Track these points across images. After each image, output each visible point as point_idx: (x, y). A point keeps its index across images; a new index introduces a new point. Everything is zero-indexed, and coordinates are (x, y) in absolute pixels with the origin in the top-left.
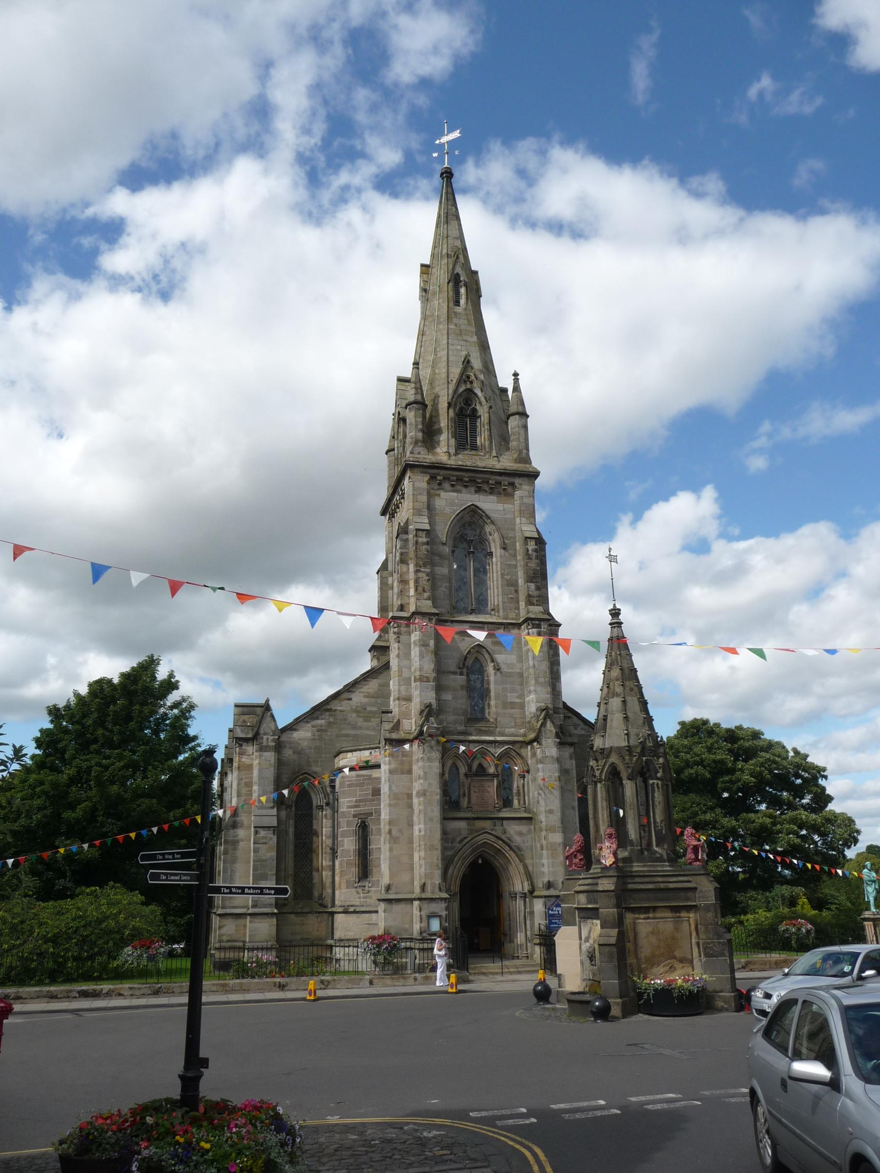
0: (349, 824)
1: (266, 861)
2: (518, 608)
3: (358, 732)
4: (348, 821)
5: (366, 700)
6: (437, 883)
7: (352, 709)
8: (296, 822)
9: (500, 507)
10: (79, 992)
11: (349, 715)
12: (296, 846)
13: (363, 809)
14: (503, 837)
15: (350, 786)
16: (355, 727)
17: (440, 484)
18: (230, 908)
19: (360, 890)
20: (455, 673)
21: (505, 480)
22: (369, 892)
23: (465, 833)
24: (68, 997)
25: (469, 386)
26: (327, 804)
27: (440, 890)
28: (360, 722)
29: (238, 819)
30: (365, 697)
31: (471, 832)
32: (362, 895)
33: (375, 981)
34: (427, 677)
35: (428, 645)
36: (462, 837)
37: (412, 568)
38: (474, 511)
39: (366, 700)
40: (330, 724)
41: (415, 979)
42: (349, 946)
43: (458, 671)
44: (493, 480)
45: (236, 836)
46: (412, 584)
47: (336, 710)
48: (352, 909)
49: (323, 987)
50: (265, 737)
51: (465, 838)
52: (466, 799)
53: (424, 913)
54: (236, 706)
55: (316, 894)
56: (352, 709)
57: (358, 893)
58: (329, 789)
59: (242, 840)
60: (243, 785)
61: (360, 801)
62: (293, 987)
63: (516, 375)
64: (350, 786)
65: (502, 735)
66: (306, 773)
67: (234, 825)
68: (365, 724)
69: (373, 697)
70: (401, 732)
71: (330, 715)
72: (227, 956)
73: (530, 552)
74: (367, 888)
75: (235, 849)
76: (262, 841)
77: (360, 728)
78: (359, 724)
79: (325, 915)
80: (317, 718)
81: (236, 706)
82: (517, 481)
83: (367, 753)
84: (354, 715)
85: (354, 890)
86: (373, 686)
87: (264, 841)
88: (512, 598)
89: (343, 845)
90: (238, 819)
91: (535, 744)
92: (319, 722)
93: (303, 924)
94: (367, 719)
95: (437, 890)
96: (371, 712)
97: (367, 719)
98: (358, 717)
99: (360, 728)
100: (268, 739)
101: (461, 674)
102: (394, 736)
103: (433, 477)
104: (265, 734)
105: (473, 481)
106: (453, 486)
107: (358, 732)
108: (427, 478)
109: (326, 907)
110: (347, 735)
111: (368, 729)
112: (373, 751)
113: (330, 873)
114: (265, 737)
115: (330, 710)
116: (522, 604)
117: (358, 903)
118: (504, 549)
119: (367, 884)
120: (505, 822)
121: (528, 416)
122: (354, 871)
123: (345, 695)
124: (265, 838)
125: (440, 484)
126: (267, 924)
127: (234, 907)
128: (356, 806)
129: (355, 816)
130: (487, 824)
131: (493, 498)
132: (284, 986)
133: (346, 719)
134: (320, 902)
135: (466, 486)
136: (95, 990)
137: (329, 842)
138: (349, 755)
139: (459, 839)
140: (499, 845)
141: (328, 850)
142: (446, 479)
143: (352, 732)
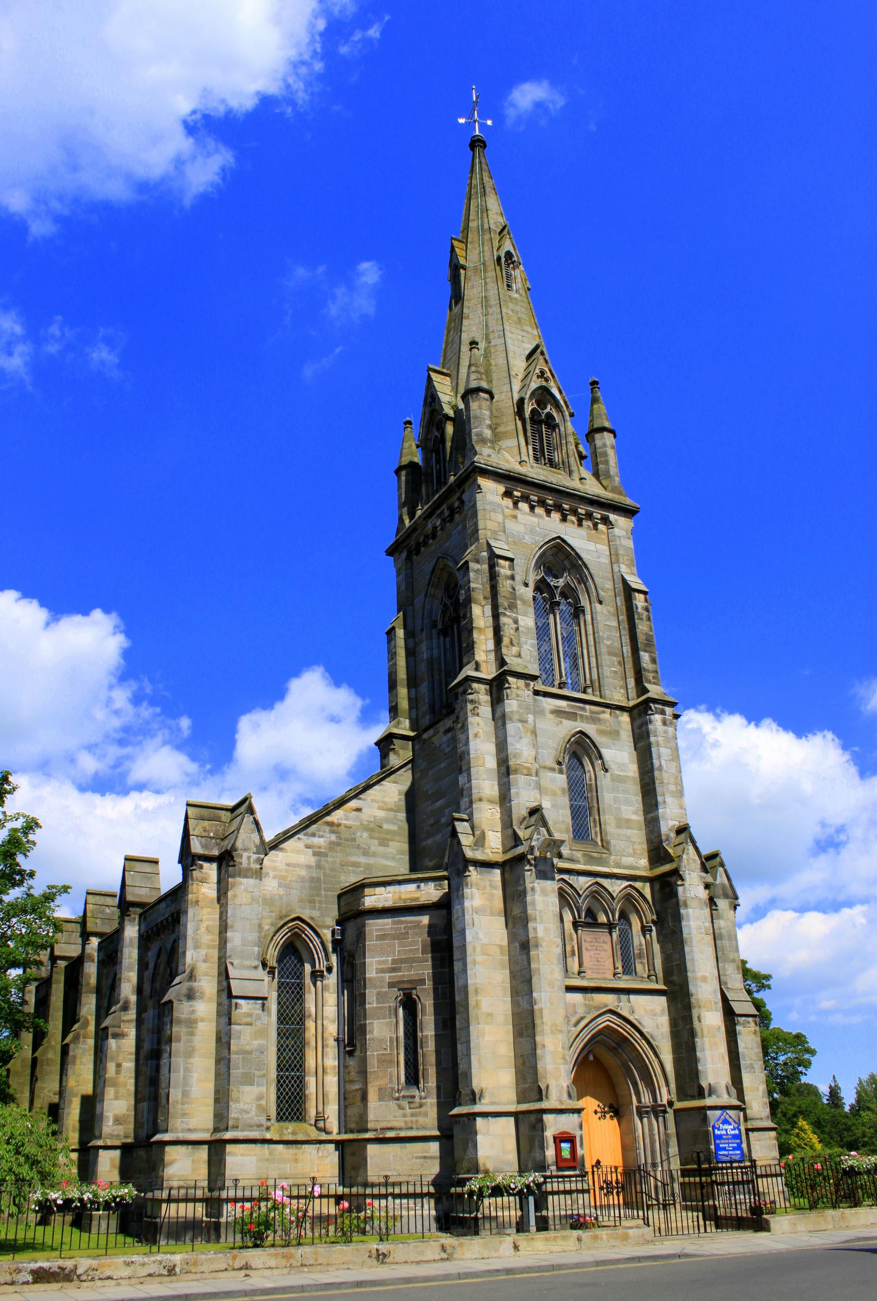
0: (380, 997)
1: (250, 1053)
3: (371, 861)
4: (378, 994)
5: (381, 814)
6: (565, 1085)
7: (362, 824)
8: (279, 995)
9: (591, 546)
10: (33, 1272)
11: (359, 834)
12: (279, 1034)
13: (407, 974)
14: (631, 1018)
15: (382, 937)
16: (366, 853)
17: (515, 504)
18: (183, 1131)
19: (405, 1103)
20: (553, 770)
22: (421, 1106)
23: (581, 1011)
24: (13, 1283)
25: (544, 384)
27: (570, 1096)
28: (374, 846)
29: (195, 985)
30: (380, 808)
31: (589, 1009)
32: (408, 1111)
33: (522, 1245)
34: (528, 769)
35: (526, 722)
36: (577, 1017)
39: (381, 814)
40: (332, 846)
41: (579, 1239)
42: (386, 1196)
43: (557, 767)
45: (193, 1012)
47: (339, 825)
49: (444, 1256)
50: (245, 855)
51: (582, 1018)
52: (576, 958)
55: (312, 1113)
56: (362, 824)
57: (400, 1107)
59: (202, 1020)
61: (402, 961)
65: (618, 866)
66: (298, 918)
68: (381, 849)
69: (391, 810)
70: (488, 851)
71: (332, 832)
72: (182, 1213)
73: (640, 610)
74: (417, 1099)
75: (192, 1034)
76: (245, 1020)
77: (374, 855)
78: (372, 848)
80: (313, 835)
82: (612, 517)
84: (365, 835)
85: (393, 1104)
87: (249, 1020)
88: (615, 672)
89: (372, 1032)
90: (195, 985)
91: (673, 879)
92: (316, 841)
93: (296, 1161)
94: (383, 843)
95: (565, 1096)
96: (388, 832)
97: (383, 843)
98: (371, 838)
99: (374, 855)
100: (249, 858)
101: (561, 772)
103: (508, 494)
104: (245, 850)
105: (558, 508)
106: (532, 508)
107: (371, 861)
109: (328, 1133)
110: (356, 865)
111: (385, 856)
112: (422, 885)
114: (245, 855)
115: (331, 824)
117: (403, 1125)
118: (601, 602)
119: (416, 1093)
120: (633, 997)
123: (353, 804)
124: (250, 1015)
126: (254, 1159)
127: (189, 1130)
128: (393, 970)
129: (391, 985)
130: (609, 1000)
131: (583, 532)
132: (385, 1255)
133: (354, 840)
134: (321, 1124)
138: (379, 890)
139: (574, 1020)
140: (625, 1030)
143: (362, 860)
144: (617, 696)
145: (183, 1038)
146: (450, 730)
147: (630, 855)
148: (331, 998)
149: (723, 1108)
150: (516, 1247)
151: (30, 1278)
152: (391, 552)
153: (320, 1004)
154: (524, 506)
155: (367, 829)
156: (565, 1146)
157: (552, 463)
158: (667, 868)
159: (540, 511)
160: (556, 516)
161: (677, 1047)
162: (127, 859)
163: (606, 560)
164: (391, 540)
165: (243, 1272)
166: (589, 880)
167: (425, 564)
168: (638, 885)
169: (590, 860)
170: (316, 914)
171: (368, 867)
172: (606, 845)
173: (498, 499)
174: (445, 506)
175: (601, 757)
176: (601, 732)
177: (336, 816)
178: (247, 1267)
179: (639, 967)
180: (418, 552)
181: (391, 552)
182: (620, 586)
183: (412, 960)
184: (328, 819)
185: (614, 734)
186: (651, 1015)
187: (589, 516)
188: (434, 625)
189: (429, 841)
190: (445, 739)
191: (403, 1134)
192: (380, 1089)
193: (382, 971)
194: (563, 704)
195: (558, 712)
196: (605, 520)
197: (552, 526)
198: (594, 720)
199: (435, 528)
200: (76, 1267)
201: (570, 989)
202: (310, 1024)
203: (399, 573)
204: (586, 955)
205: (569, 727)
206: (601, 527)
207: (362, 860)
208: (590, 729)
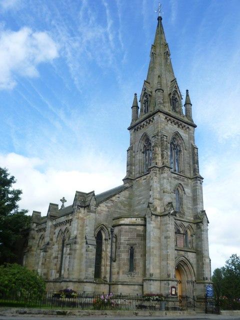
2: (190, 173)
3: (121, 211)
10: (57, 312)
16: (120, 209)
17: (168, 121)
19: (129, 275)
21: (187, 126)
24: (52, 314)
26: (110, 239)
28: (122, 207)
29: (77, 240)
33: (167, 314)
37: (160, 149)
38: (177, 134)
39: (124, 199)
44: (184, 124)
46: (160, 155)
48: (126, 283)
53: (170, 286)
54: (77, 192)
55: (103, 276)
57: (128, 276)
58: (110, 233)
60: (79, 226)
62: (140, 314)
63: (187, 91)
64: (126, 232)
66: (103, 225)
67: (75, 243)
75: (75, 253)
77: (122, 210)
79: (107, 285)
81: (77, 192)
83: (134, 219)
85: (126, 275)
86: (126, 193)
90: (77, 240)
91: (200, 224)
92: (109, 205)
99: (122, 210)
102: (155, 213)
103: (166, 118)
106: (171, 123)
107: (121, 211)
108: (165, 117)
110: (117, 212)
113: (109, 268)
115: (112, 200)
116: (192, 172)
119: (133, 273)
121: (191, 105)
122: (127, 268)
123: (117, 196)
124: (92, 249)
125: (168, 121)
128: (128, 240)
129: (127, 244)
135: (175, 124)
136: (64, 312)
137: (109, 254)
138: (125, 219)
141: (109, 258)
142: (170, 120)
143: (119, 211)
144: (188, 175)
145: (73, 254)
146: (145, 179)
147: (189, 217)
148: (109, 246)
149: (209, 283)
150: (166, 314)
151: (56, 313)
152: (129, 129)
153: (106, 248)
154: (169, 122)
155: (120, 203)
156: (174, 289)
157: (175, 111)
158: (199, 221)
159: (173, 124)
160: (177, 126)
161: (198, 267)
162: (50, 204)
163: (187, 139)
164: (129, 125)
165: (105, 316)
166: (188, 224)
167: (140, 134)
168: (191, 224)
169: (180, 217)
170: (107, 224)
171: (120, 213)
172: (184, 214)
173: (164, 120)
174: (148, 119)
175: (184, 190)
176: (185, 184)
177: (114, 198)
178: (106, 314)
179: (189, 246)
180: (137, 131)
181: (129, 129)
182: (191, 146)
183: (134, 238)
184: (111, 199)
185: (187, 185)
186: (191, 257)
187: (185, 126)
188: (141, 151)
189: (137, 208)
190: (144, 181)
191: (129, 283)
192: (123, 271)
193: (124, 240)
194: (176, 175)
195: (175, 178)
196: (188, 128)
197: (175, 128)
198: (183, 181)
199: (144, 124)
200: (67, 312)
201: (176, 250)
202: (103, 253)
203: (131, 135)
204: (178, 242)
205: (177, 182)
206: (187, 130)
207: (119, 211)
208: (182, 183)
